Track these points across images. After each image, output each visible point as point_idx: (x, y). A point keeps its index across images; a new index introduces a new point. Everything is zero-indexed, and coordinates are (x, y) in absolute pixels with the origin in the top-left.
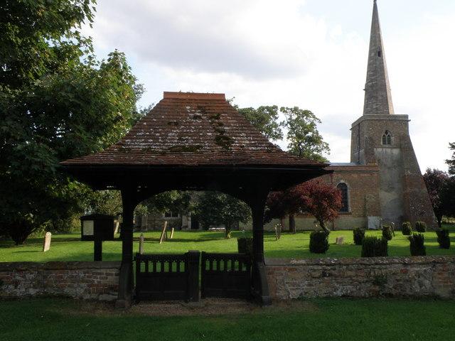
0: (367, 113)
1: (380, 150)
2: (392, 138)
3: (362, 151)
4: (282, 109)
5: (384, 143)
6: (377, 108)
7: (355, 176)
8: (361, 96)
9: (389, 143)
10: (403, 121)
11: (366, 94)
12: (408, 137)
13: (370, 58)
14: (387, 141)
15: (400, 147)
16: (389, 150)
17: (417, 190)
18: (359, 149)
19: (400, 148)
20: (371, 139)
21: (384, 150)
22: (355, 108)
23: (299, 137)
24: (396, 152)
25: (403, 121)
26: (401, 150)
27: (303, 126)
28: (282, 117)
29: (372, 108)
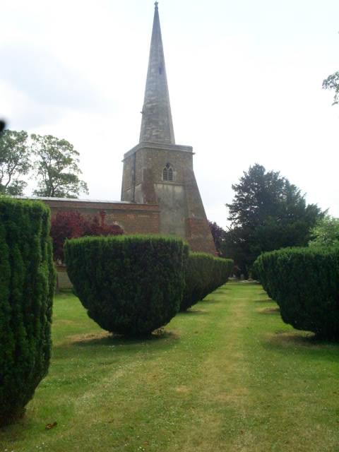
0: (148, 103)
1: (160, 186)
2: (175, 173)
3: (138, 187)
4: (33, 136)
5: (165, 178)
6: (157, 136)
7: (132, 217)
8: (138, 119)
9: (171, 179)
10: (187, 154)
11: (143, 118)
12: (192, 174)
13: (150, 74)
14: (168, 176)
15: (183, 184)
16: (170, 188)
17: (201, 236)
18: (134, 184)
19: (184, 186)
20: (150, 171)
21: (165, 186)
22: (130, 136)
23: (53, 173)
24: (179, 190)
25: (187, 154)
26: (185, 189)
27: (58, 157)
28: (29, 142)
29: (151, 135)
